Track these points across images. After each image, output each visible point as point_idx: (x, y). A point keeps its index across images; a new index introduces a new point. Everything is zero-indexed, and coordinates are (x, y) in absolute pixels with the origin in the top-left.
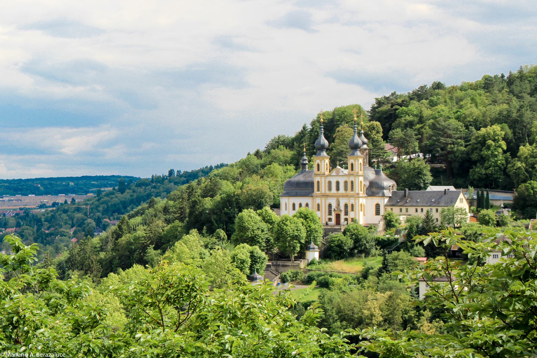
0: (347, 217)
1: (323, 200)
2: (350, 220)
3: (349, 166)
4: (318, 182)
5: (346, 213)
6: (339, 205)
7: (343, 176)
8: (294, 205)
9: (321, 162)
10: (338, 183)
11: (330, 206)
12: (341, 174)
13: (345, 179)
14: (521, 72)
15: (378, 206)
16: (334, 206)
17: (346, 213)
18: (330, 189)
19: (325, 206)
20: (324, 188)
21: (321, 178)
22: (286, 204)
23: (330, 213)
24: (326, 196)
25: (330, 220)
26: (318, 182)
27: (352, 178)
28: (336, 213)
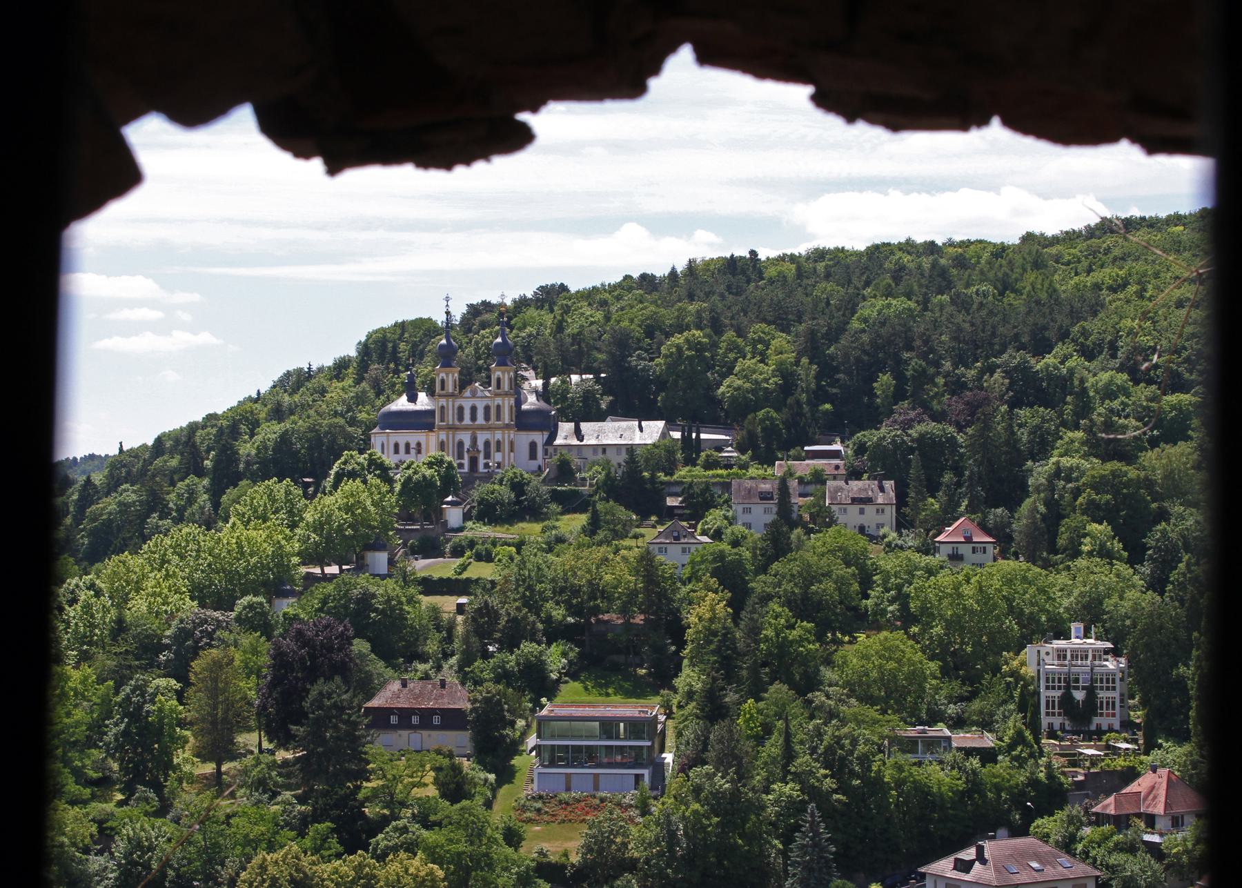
3: (494, 382)
5: (487, 456)
6: (474, 440)
8: (396, 446)
10: (474, 409)
11: (461, 444)
12: (479, 394)
14: (691, 263)
15: (533, 446)
16: (467, 445)
17: (487, 456)
18: (461, 418)
22: (383, 445)
23: (460, 456)
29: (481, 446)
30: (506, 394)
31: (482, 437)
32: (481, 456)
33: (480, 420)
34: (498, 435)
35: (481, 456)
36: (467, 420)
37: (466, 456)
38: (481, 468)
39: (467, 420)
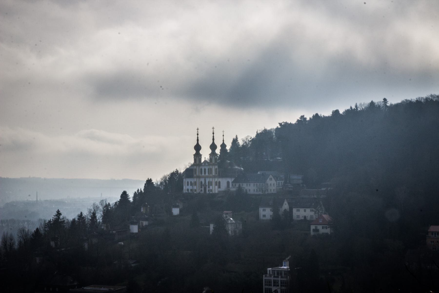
5: (209, 187)
8: (188, 182)
10: (205, 169)
11: (201, 182)
13: (208, 167)
15: (228, 183)
16: (203, 183)
23: (201, 188)
24: (199, 177)
25: (201, 190)
27: (211, 167)
29: (207, 184)
32: (207, 187)
33: (207, 174)
34: (211, 180)
35: (207, 187)
36: (203, 174)
38: (207, 191)
39: (203, 174)
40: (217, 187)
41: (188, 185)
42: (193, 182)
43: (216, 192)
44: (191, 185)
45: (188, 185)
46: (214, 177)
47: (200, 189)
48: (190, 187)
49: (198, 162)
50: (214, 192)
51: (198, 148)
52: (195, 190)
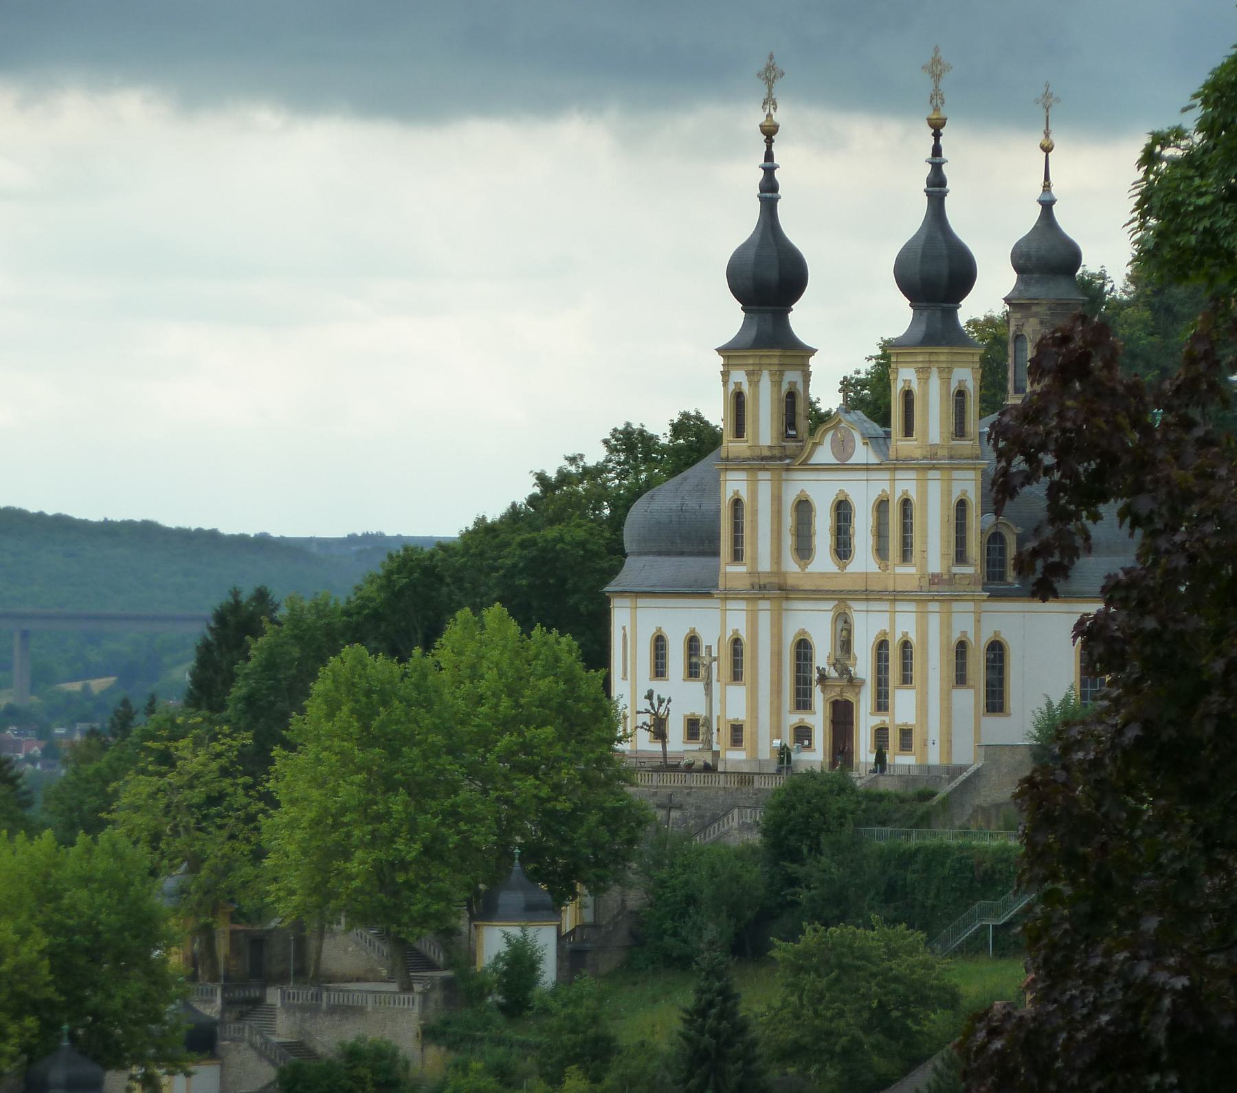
0: (887, 719)
1: (765, 619)
2: (894, 739)
4: (737, 503)
5: (882, 704)
6: (845, 645)
7: (867, 467)
8: (659, 644)
9: (754, 384)
10: (843, 510)
11: (803, 649)
13: (879, 485)
16: (822, 657)
17: (882, 704)
18: (804, 550)
19: (777, 655)
20: (764, 549)
21: (753, 482)
23: (803, 702)
24: (776, 591)
25: (803, 734)
26: (737, 503)
27: (906, 484)
28: (834, 694)
30: (926, 464)
31: (869, 625)
34: (905, 623)
36: (823, 559)
37: (819, 699)
39: (823, 559)
40: (969, 699)
41: (659, 670)
42: (708, 638)
43: (966, 755)
44: (692, 671)
45: (659, 670)
46: (938, 591)
47: (794, 719)
48: (684, 697)
49: (765, 428)
50: (934, 757)
51: (769, 280)
52: (737, 729)
